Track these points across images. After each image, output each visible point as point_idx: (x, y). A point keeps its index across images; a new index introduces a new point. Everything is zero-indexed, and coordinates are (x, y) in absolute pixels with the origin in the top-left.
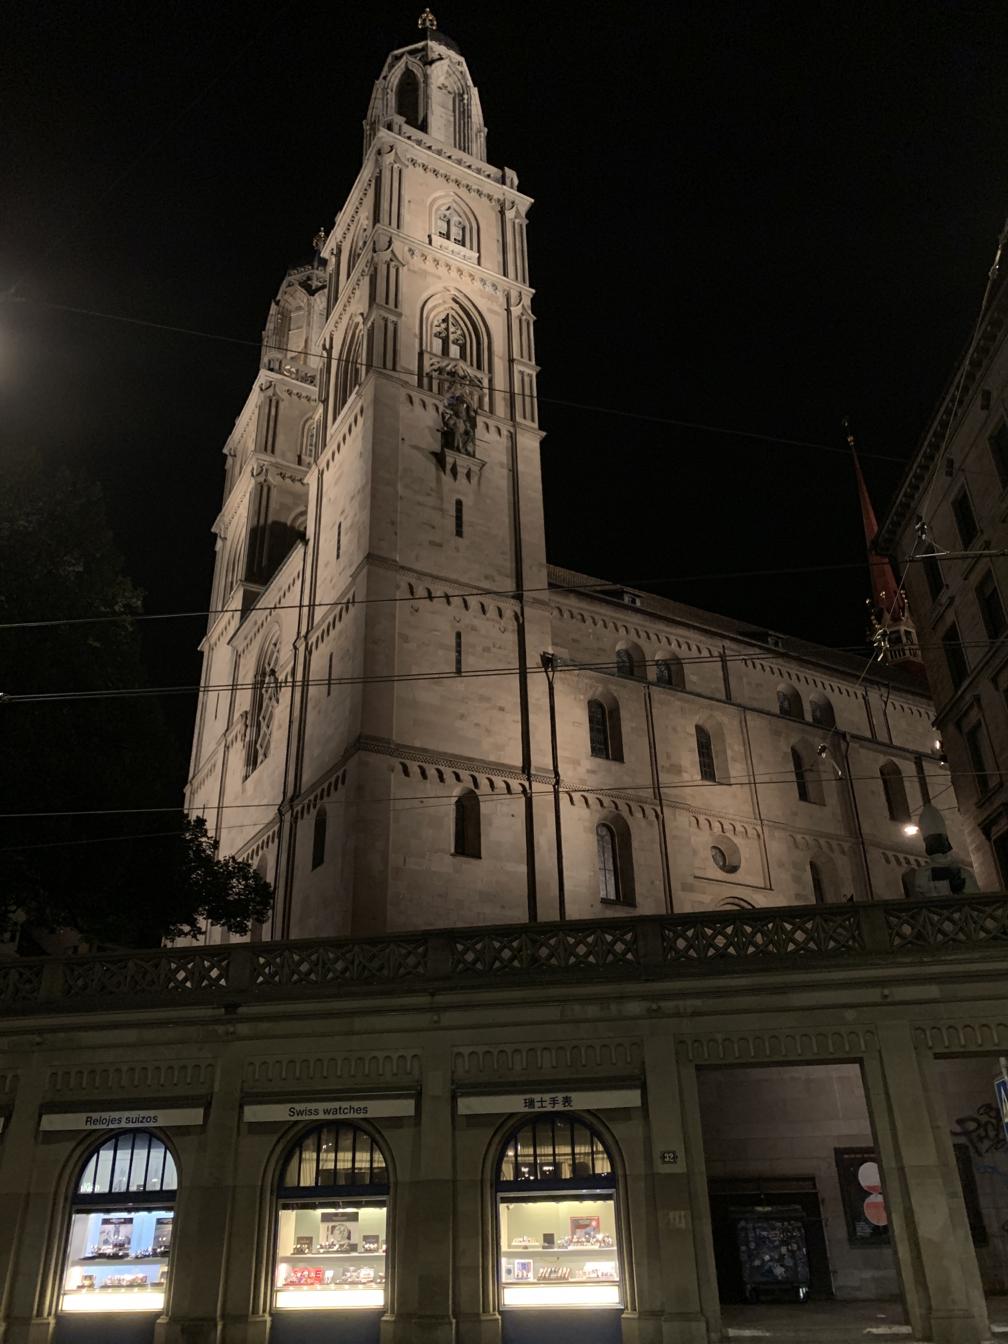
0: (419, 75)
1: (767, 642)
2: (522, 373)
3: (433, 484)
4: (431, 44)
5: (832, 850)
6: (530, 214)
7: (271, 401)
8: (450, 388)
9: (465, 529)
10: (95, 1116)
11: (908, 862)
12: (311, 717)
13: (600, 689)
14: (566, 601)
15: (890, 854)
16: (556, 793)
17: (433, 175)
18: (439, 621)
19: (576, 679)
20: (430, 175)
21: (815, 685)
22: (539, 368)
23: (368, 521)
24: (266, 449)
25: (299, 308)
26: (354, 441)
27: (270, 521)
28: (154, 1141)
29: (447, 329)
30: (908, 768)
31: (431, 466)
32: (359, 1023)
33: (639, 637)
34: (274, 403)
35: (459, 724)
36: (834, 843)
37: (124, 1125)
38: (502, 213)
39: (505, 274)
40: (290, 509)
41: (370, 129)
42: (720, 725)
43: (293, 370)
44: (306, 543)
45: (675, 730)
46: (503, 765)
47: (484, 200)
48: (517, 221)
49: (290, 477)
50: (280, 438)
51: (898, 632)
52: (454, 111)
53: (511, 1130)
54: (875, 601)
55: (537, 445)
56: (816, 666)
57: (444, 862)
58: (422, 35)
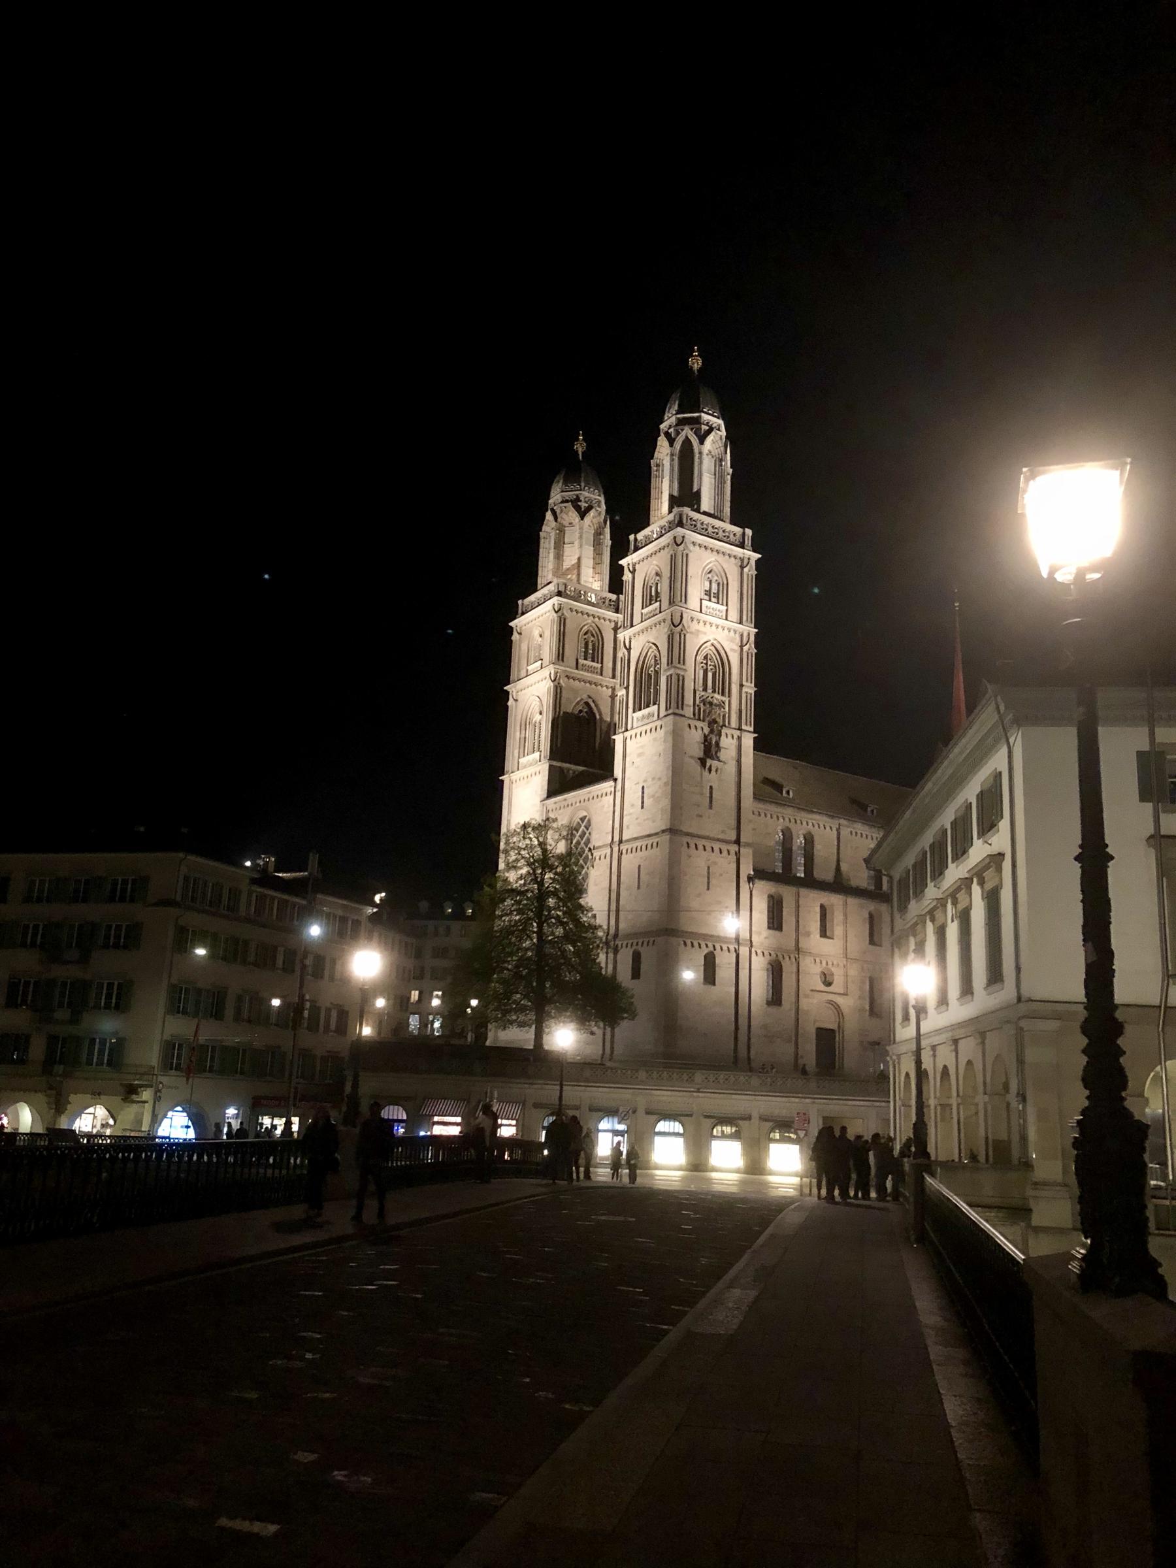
6: (758, 561)
18: (698, 861)
26: (655, 740)
38: (742, 567)
42: (832, 905)
44: (615, 780)
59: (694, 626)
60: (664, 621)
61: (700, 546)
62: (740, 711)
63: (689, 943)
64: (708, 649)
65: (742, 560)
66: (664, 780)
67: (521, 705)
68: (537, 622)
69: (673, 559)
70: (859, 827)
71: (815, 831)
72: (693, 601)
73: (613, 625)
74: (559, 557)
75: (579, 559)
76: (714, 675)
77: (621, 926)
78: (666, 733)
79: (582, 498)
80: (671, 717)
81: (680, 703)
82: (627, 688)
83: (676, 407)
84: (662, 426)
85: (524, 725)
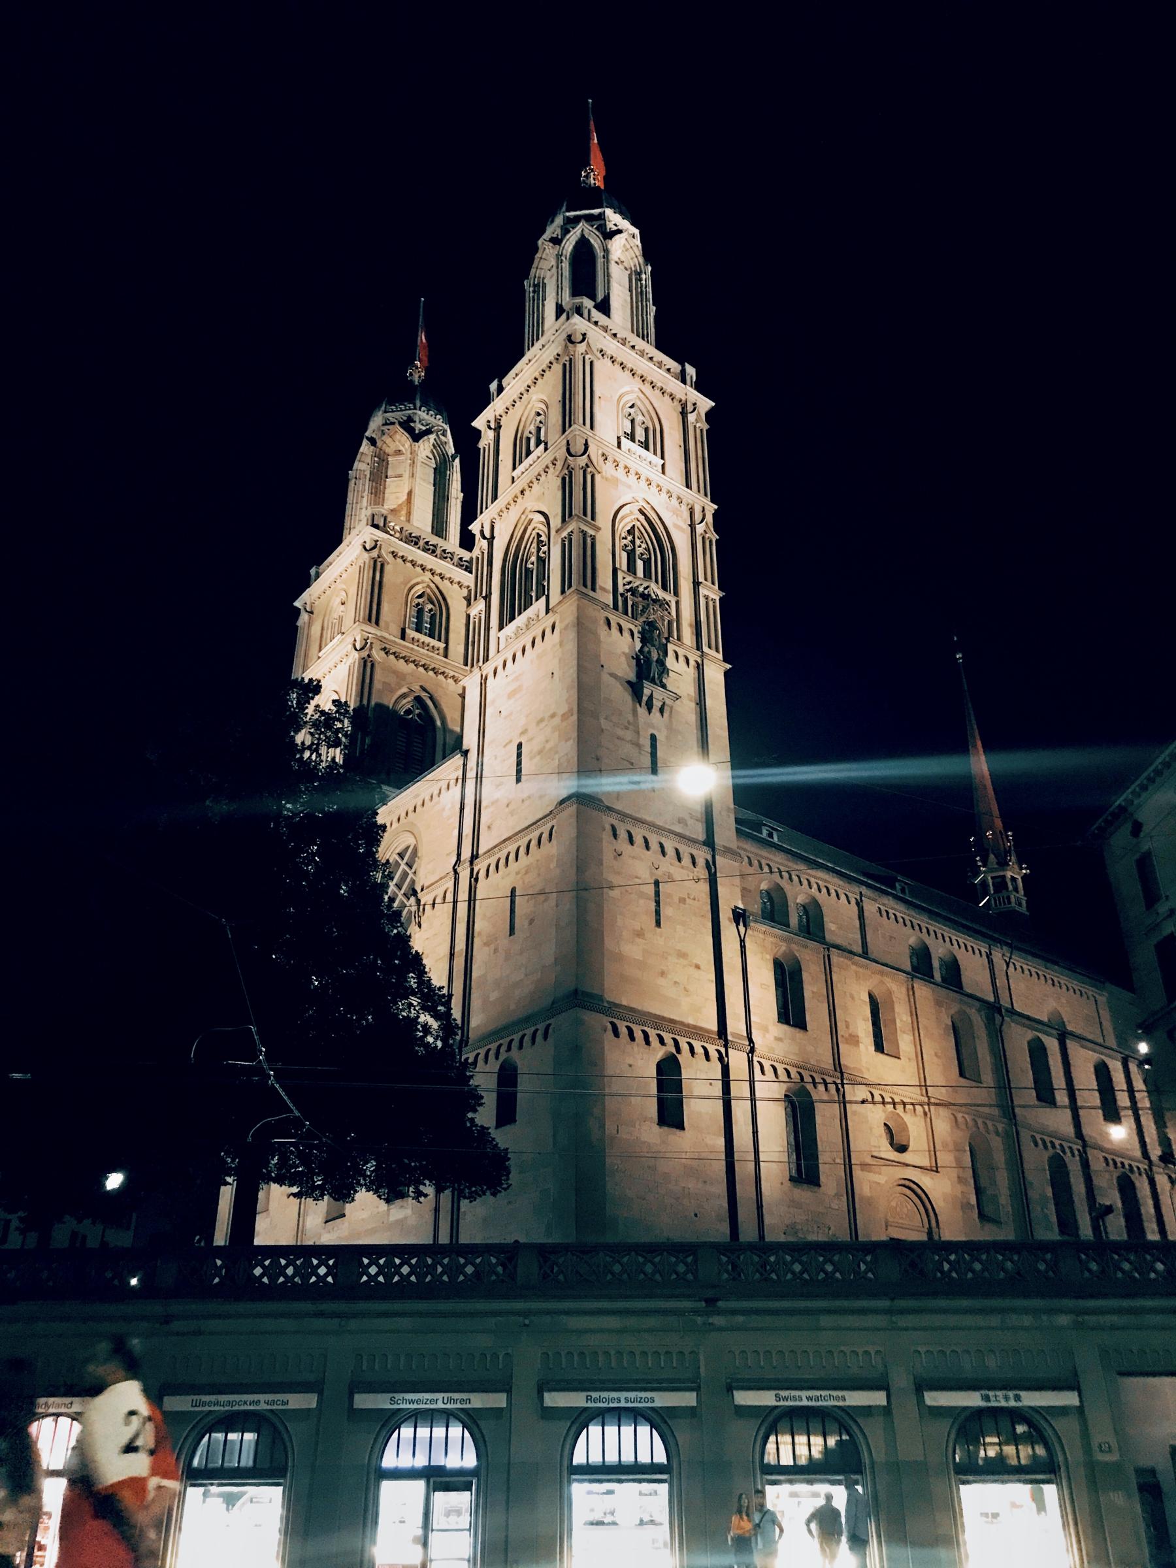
0: (596, 246)
1: (894, 888)
2: (707, 598)
3: (630, 717)
4: (609, 212)
5: (988, 1132)
7: (375, 562)
8: (643, 611)
10: (595, 1395)
11: (1053, 1146)
13: (784, 947)
14: (796, 867)
15: (1038, 1137)
16: (750, 1062)
17: (610, 362)
19: (762, 936)
20: (617, 366)
21: (945, 943)
22: (722, 594)
24: (370, 620)
25: (399, 452)
26: (539, 657)
27: (373, 703)
28: (640, 1419)
29: (633, 542)
30: (1052, 1044)
31: (626, 697)
32: (825, 1321)
33: (782, 877)
34: (379, 564)
35: (661, 981)
36: (989, 1124)
37: (623, 1404)
38: (684, 414)
39: (688, 486)
40: (392, 691)
41: (534, 292)
42: (890, 993)
43: (397, 528)
44: (465, 753)
45: (852, 997)
46: (701, 1029)
47: (667, 397)
48: (698, 425)
49: (433, 669)
50: (386, 607)
51: (1004, 877)
52: (631, 290)
53: (778, 1421)
54: (981, 837)
55: (721, 679)
56: (947, 920)
57: (651, 1133)
58: (593, 198)
59: (607, 469)
63: (623, 1031)
66: (564, 708)
68: (340, 585)
69: (567, 372)
70: (889, 903)
71: (822, 897)
73: (465, 592)
74: (378, 494)
75: (410, 494)
76: (647, 563)
77: (475, 1021)
81: (589, 578)
82: (487, 598)
83: (564, 209)
84: (540, 242)
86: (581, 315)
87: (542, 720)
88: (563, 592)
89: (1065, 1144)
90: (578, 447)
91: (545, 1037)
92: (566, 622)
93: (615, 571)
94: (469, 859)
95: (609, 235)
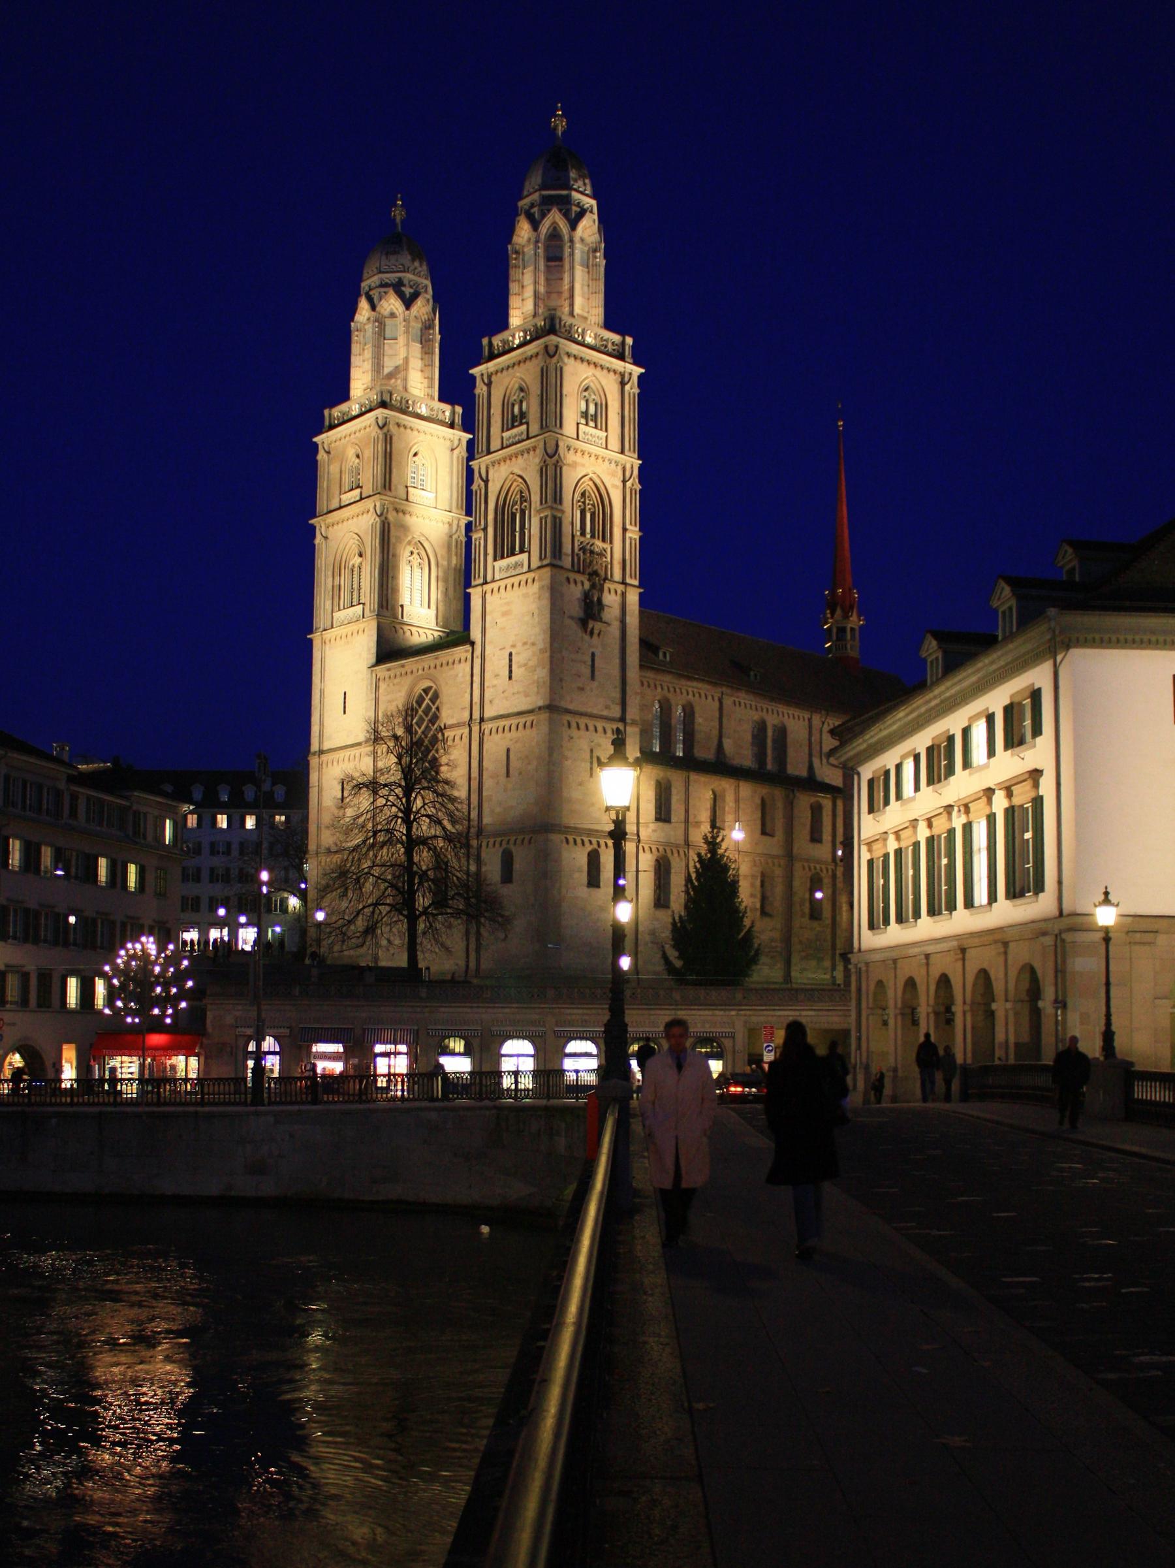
2: (631, 539)
6: (640, 377)
9: (597, 673)
12: (488, 783)
13: (662, 774)
16: (637, 847)
20: (579, 361)
23: (547, 679)
29: (584, 503)
38: (623, 384)
42: (724, 790)
44: (473, 644)
57: (583, 891)
59: (570, 457)
60: (534, 448)
61: (575, 357)
62: (624, 561)
63: (571, 841)
64: (586, 485)
65: (622, 375)
66: (541, 645)
67: (332, 544)
69: (544, 373)
70: (744, 697)
71: (695, 700)
72: (569, 428)
76: (593, 515)
77: (486, 820)
78: (541, 588)
79: (406, 282)
80: (548, 569)
81: (557, 551)
82: (485, 529)
84: (521, 204)
85: (337, 569)
86: (556, 334)
87: (525, 644)
88: (541, 559)
89: (823, 867)
90: (550, 451)
91: (530, 842)
92: (544, 583)
93: (573, 536)
94: (478, 719)
95: (573, 225)
